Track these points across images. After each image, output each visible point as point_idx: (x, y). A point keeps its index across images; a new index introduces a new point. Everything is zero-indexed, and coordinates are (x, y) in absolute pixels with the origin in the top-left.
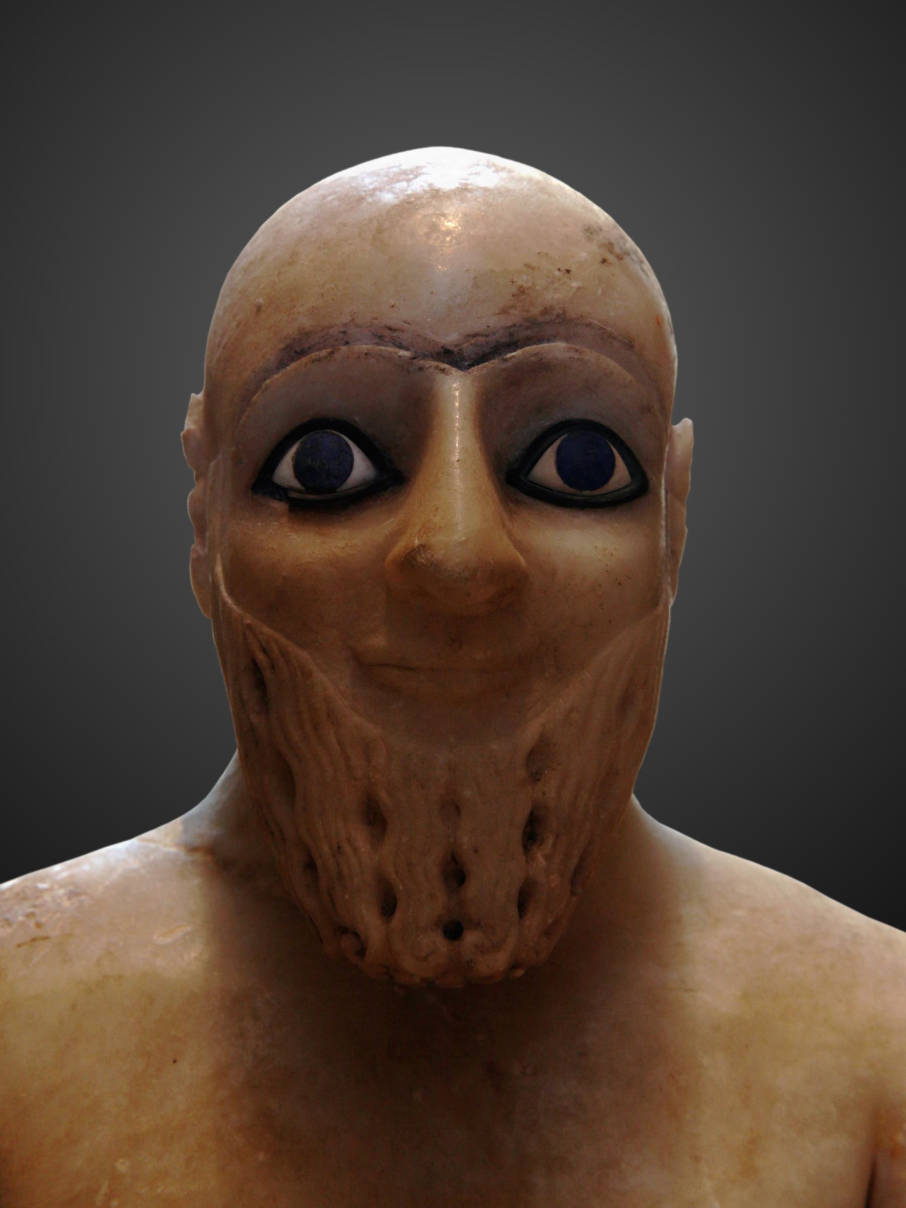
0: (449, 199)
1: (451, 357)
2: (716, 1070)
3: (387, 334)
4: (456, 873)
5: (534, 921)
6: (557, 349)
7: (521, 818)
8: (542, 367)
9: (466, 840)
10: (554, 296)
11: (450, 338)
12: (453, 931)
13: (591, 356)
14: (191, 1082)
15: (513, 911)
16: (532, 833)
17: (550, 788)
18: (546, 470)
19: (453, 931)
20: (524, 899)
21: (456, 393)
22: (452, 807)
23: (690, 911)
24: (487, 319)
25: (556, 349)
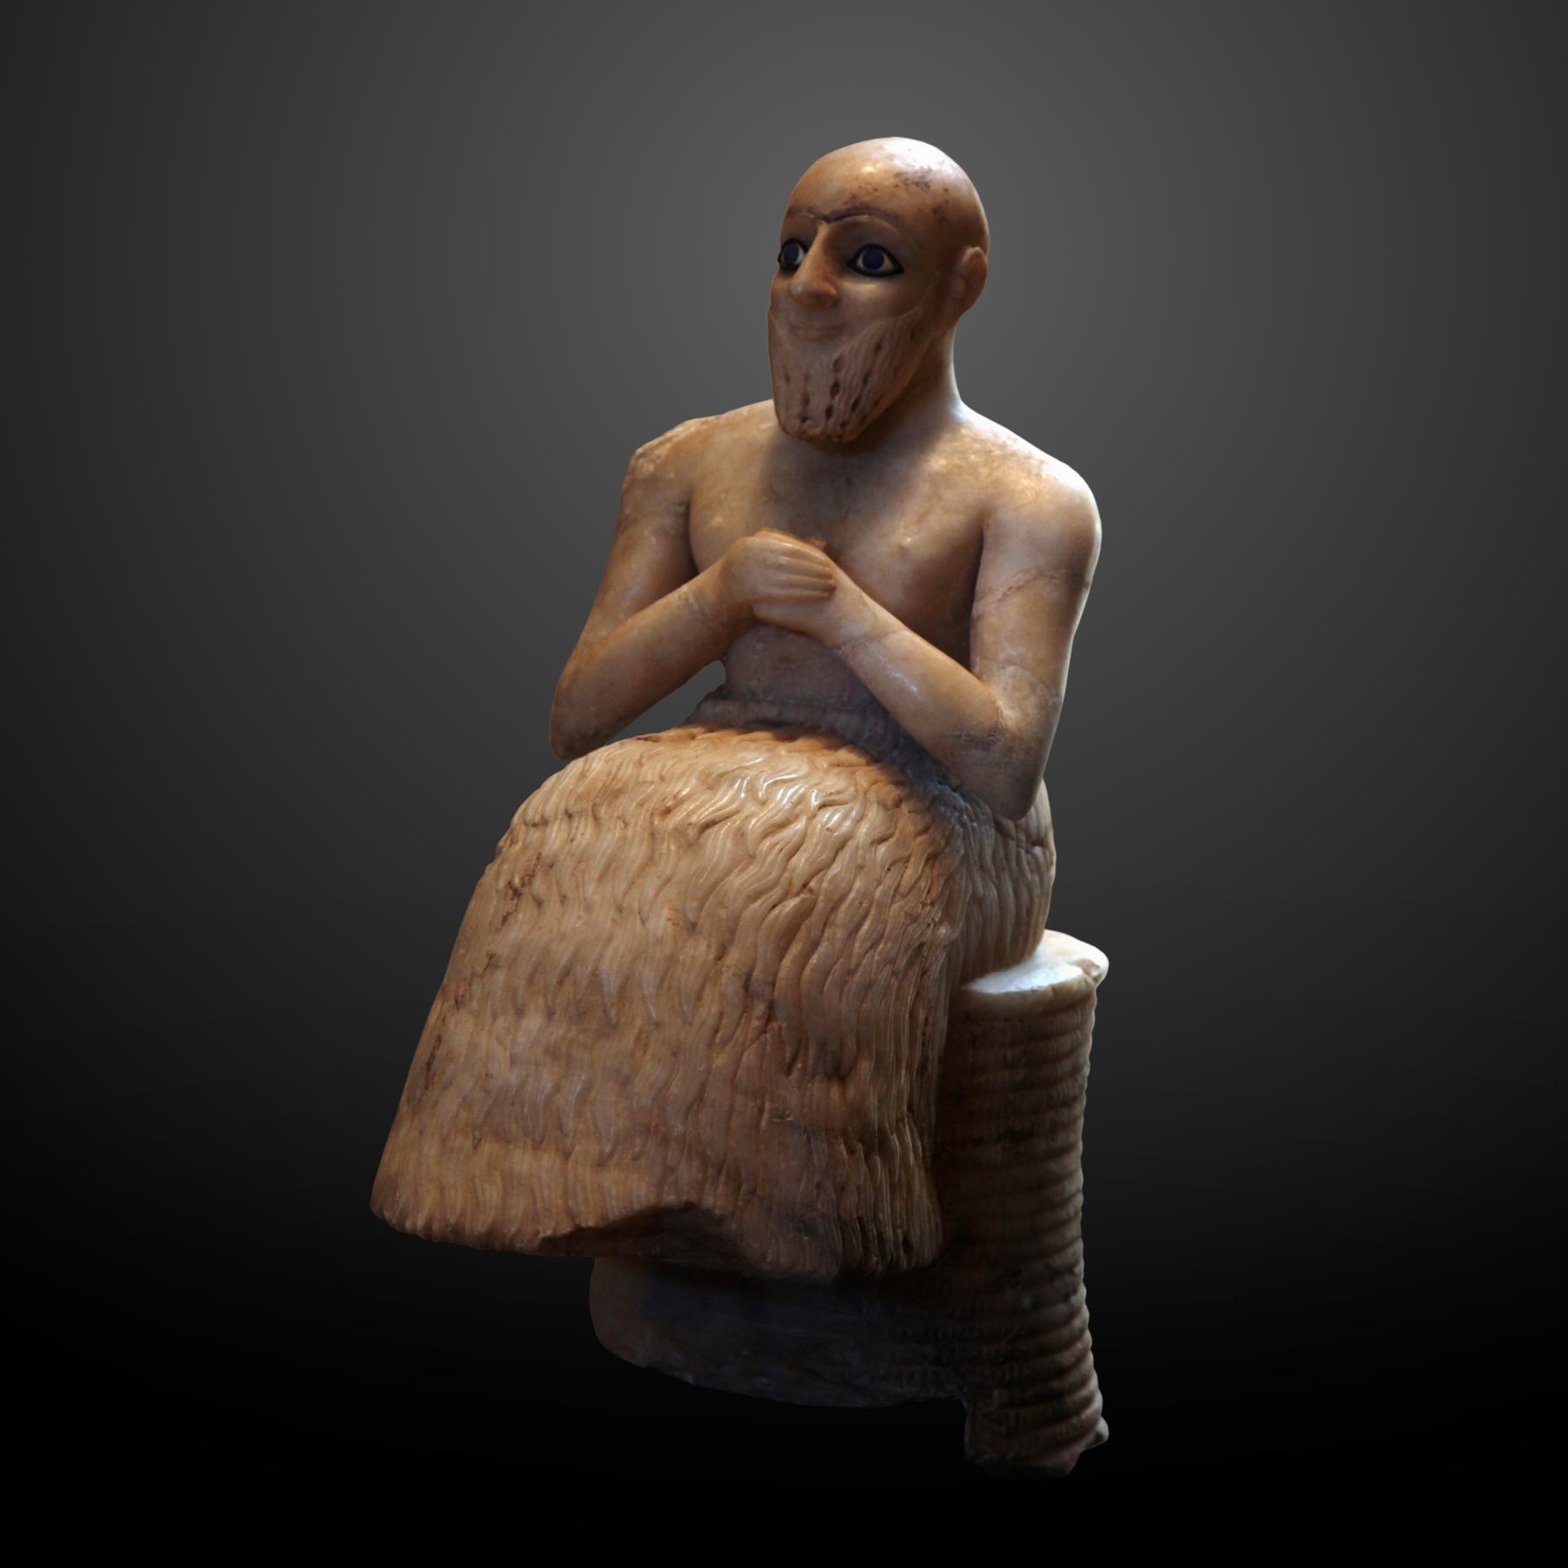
0: (912, 158)
1: (827, 219)
2: (925, 488)
3: (810, 210)
4: (806, 400)
5: (833, 420)
6: (864, 218)
7: (831, 382)
8: (855, 225)
9: (809, 389)
10: (867, 199)
11: (827, 212)
12: (804, 420)
13: (876, 220)
14: (752, 475)
15: (823, 415)
16: (835, 389)
17: (842, 375)
18: (860, 262)
19: (804, 420)
20: (829, 412)
21: (823, 231)
22: (807, 378)
23: (947, 436)
24: (839, 206)
25: (864, 218)
